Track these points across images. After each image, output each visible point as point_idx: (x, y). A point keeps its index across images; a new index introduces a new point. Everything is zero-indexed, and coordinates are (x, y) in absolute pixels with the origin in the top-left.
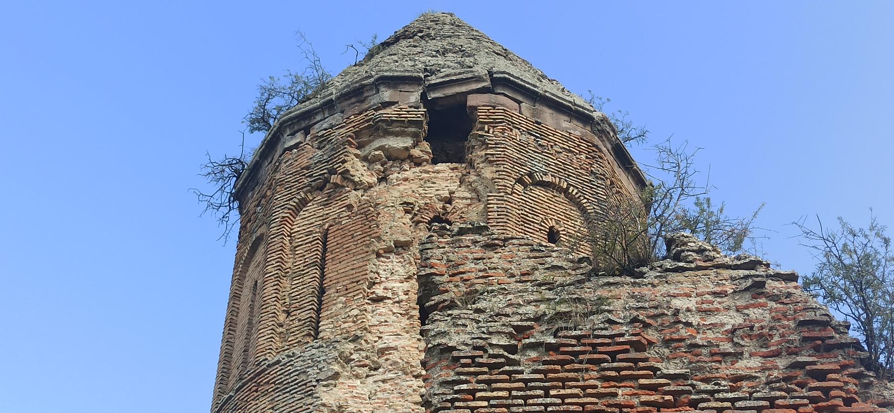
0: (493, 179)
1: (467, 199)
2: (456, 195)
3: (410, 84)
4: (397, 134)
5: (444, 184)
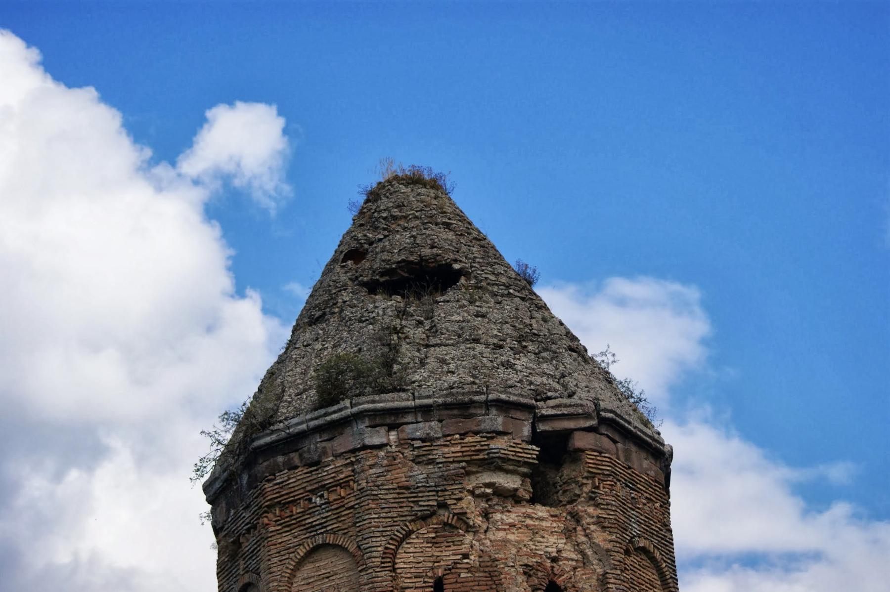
0: (608, 550)
1: (572, 560)
2: (564, 555)
3: (521, 411)
4: (507, 472)
5: (552, 539)
